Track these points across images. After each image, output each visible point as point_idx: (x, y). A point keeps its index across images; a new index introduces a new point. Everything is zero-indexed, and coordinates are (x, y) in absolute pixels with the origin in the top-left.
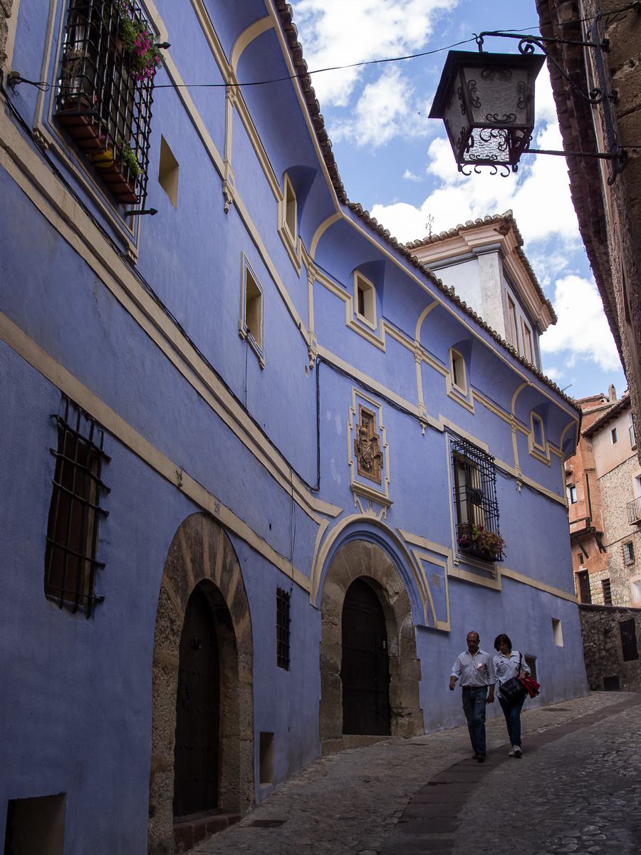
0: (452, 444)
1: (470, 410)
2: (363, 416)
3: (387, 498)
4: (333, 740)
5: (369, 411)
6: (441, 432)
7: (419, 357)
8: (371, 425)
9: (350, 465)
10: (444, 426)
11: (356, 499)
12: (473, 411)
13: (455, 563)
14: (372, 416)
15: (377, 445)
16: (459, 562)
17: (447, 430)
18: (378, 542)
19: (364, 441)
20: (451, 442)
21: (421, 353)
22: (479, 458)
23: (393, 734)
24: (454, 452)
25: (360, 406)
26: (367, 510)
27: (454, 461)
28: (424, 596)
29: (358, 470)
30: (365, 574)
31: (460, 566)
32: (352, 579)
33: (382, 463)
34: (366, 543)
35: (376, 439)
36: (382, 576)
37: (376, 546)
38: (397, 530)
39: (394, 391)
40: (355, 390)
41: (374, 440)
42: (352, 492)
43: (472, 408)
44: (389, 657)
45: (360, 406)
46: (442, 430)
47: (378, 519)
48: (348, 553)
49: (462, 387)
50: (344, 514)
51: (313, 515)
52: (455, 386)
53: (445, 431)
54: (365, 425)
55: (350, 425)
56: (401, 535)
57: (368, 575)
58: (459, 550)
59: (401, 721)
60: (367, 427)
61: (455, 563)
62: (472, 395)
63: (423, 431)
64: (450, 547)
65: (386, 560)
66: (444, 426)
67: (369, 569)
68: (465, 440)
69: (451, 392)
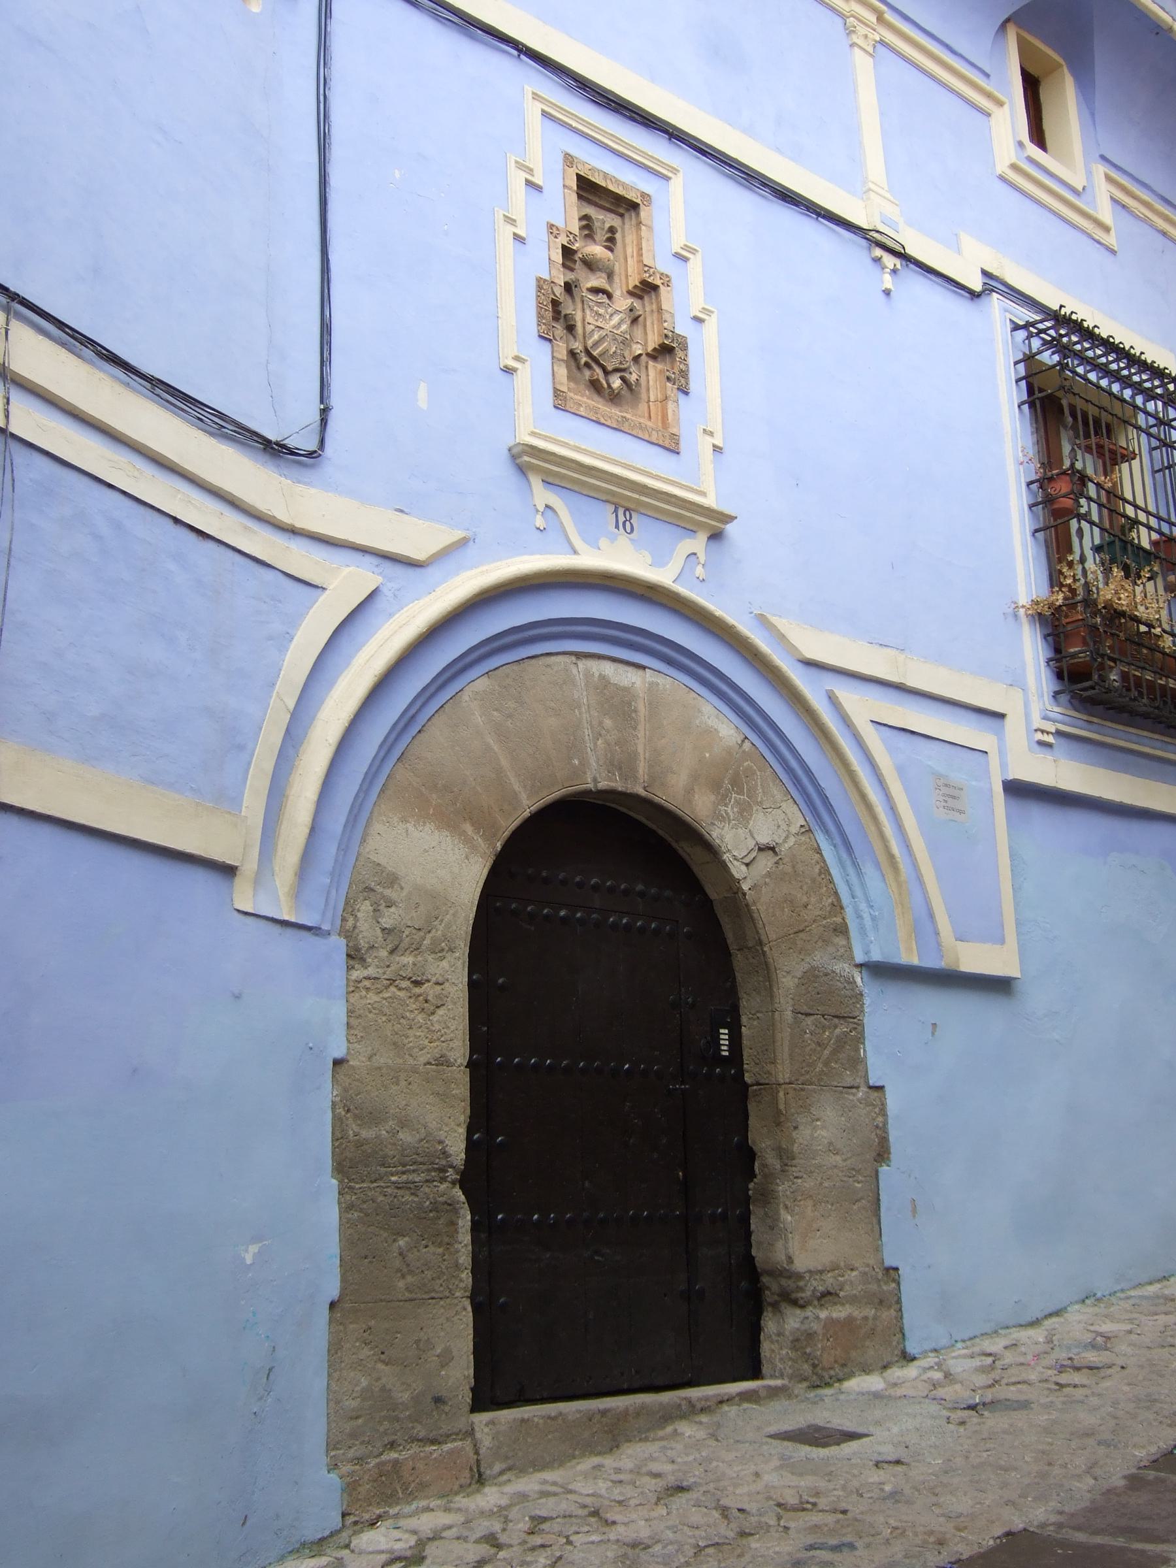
0: (1022, 334)
1: (1099, 234)
2: (580, 197)
3: (710, 501)
4: (415, 1449)
5: (618, 182)
6: (974, 295)
7: (861, 30)
8: (630, 238)
9: (508, 371)
10: (985, 273)
11: (542, 495)
12: (1111, 240)
13: (1039, 736)
14: (634, 206)
15: (660, 310)
16: (1059, 733)
17: (993, 283)
18: (670, 662)
19: (596, 291)
20: (1016, 327)
21: (873, 18)
22: (1138, 388)
23: (765, 1369)
24: (1029, 359)
25: (569, 160)
26: (603, 542)
27: (1030, 390)
28: (891, 857)
29: (557, 393)
30: (603, 785)
31: (1060, 744)
32: (528, 805)
33: (684, 374)
34: (608, 668)
35: (655, 288)
36: (689, 791)
37: (661, 680)
38: (762, 620)
39: (749, 131)
40: (536, 96)
41: (647, 289)
42: (522, 470)
43: (1107, 229)
44: (746, 1086)
45: (569, 160)
46: (977, 286)
47: (664, 576)
48: (511, 704)
49: (1064, 158)
50: (471, 550)
51: (258, 542)
52: (1034, 151)
53: (988, 290)
54: (601, 236)
55: (510, 221)
56: (781, 638)
57: (619, 786)
58: (1056, 695)
59: (793, 1320)
60: (611, 243)
61: (1039, 736)
62: (1102, 192)
63: (888, 281)
64: (1016, 682)
65: (711, 732)
66: (985, 273)
67: (626, 766)
68: (1060, 319)
69: (1014, 167)
